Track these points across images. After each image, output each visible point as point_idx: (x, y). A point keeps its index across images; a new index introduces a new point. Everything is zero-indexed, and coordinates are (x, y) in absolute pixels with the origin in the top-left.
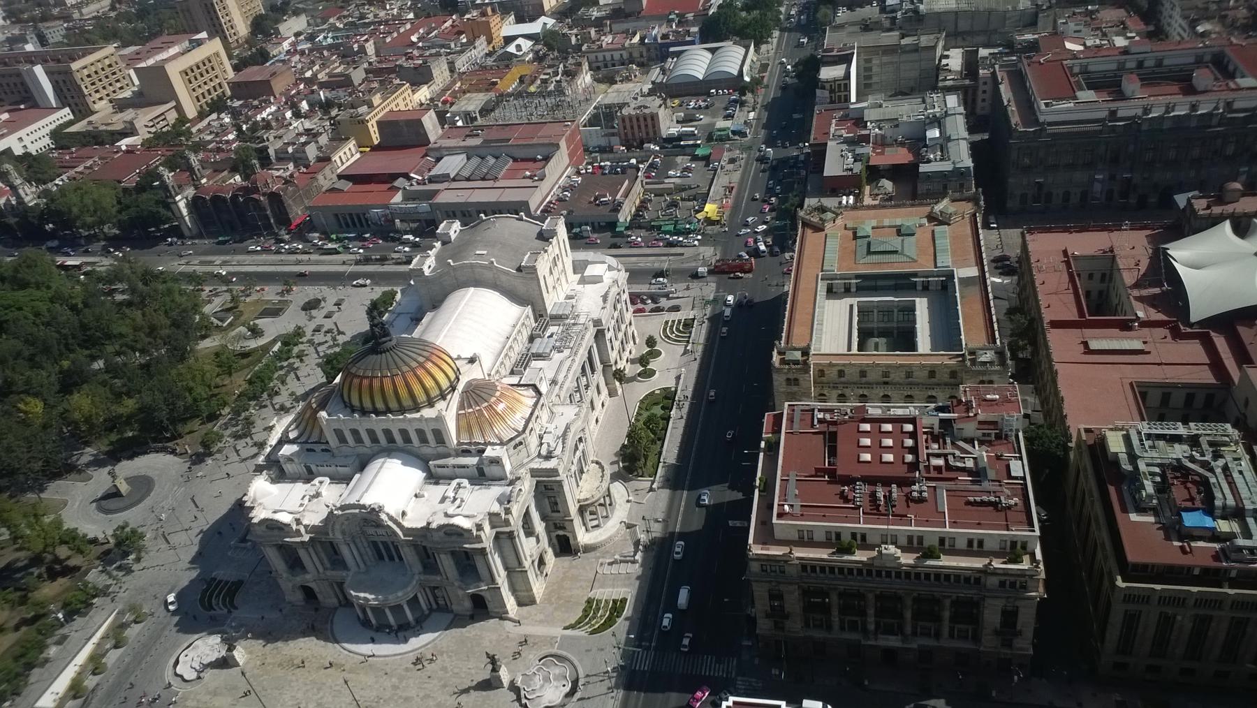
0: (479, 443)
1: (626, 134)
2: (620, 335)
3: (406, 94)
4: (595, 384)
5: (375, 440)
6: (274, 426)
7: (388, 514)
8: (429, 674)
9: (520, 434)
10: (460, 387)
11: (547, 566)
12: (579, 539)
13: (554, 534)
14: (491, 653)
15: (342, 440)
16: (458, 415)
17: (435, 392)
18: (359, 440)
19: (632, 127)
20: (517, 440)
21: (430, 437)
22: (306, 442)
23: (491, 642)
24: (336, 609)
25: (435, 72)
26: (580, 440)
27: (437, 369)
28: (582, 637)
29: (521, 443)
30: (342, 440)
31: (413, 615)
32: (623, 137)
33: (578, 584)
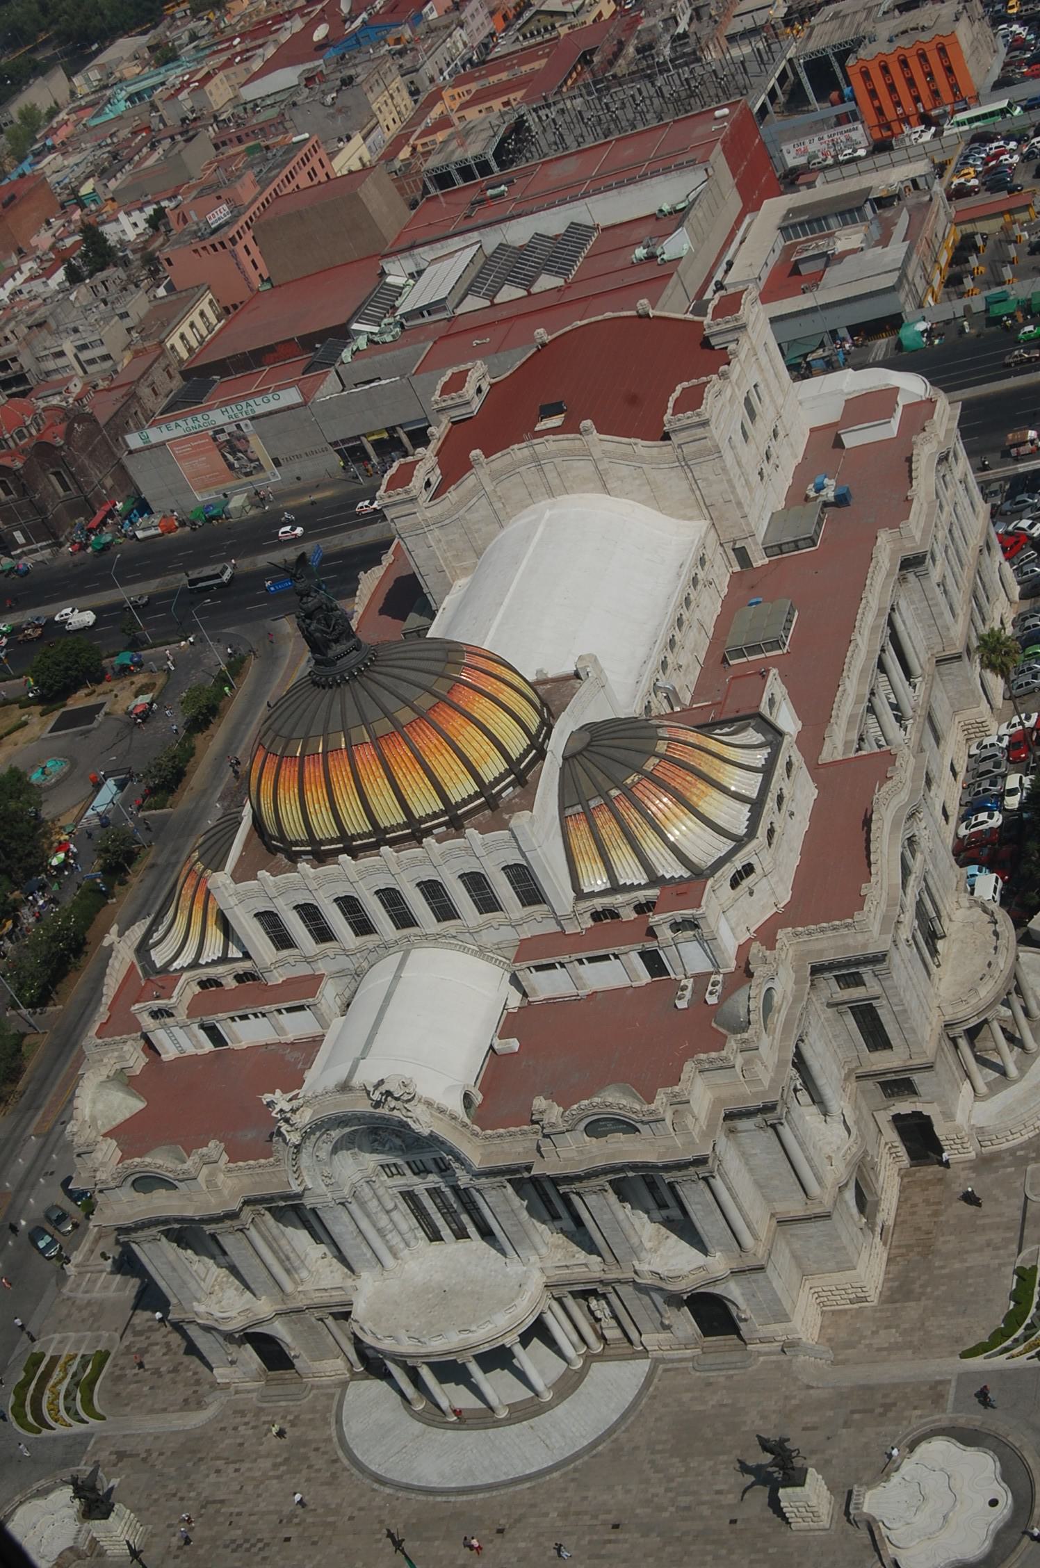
0: (640, 887)
1: (880, 111)
2: (967, 575)
3: (314, 162)
4: (922, 712)
5: (363, 926)
6: (111, 948)
7: (429, 1104)
8: (612, 1518)
9: (740, 842)
10: (557, 745)
11: (884, 1206)
12: (960, 1118)
13: (884, 1118)
14: (772, 1435)
15: (282, 940)
16: (563, 820)
17: (492, 767)
18: (323, 934)
19: (892, 88)
20: (738, 863)
21: (503, 889)
22: (194, 965)
23: (764, 1417)
24: (344, 1385)
25: (377, 101)
26: (911, 841)
27: (486, 702)
28: (1018, 1372)
29: (748, 869)
30: (282, 940)
31: (542, 1373)
32: (873, 119)
33: (980, 1239)
